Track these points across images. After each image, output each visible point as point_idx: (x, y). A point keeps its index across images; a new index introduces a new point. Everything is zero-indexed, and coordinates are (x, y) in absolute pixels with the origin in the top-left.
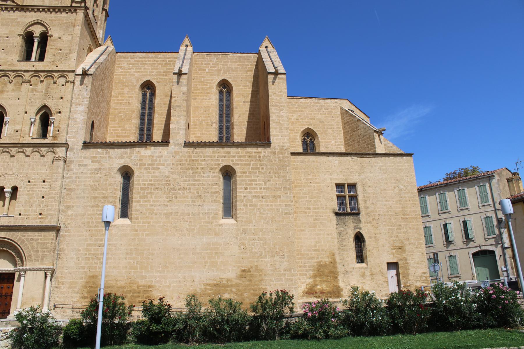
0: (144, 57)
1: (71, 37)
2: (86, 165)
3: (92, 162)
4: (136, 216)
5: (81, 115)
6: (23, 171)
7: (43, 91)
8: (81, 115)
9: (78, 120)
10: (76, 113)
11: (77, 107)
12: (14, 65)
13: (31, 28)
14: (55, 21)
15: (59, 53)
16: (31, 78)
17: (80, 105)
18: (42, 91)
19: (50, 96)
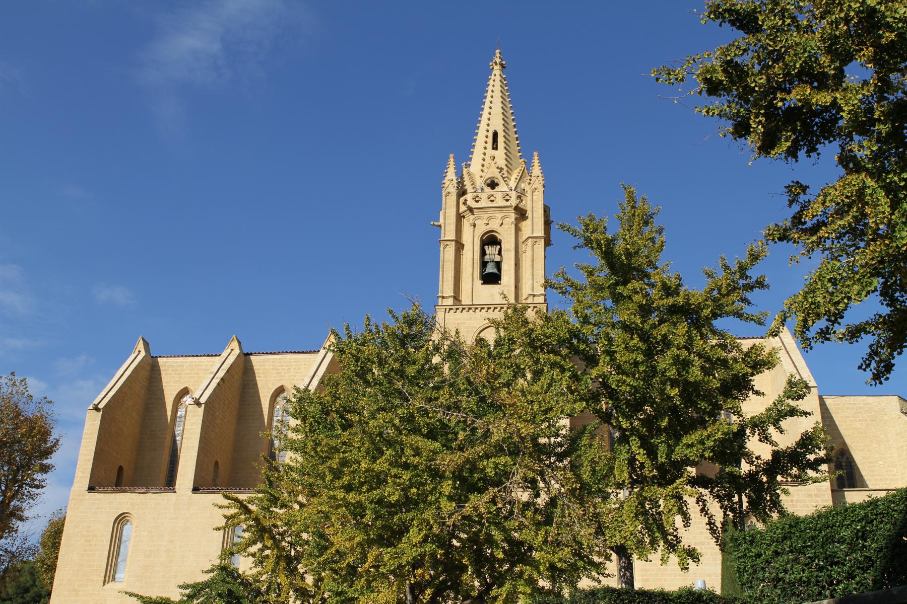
4: (645, 577)
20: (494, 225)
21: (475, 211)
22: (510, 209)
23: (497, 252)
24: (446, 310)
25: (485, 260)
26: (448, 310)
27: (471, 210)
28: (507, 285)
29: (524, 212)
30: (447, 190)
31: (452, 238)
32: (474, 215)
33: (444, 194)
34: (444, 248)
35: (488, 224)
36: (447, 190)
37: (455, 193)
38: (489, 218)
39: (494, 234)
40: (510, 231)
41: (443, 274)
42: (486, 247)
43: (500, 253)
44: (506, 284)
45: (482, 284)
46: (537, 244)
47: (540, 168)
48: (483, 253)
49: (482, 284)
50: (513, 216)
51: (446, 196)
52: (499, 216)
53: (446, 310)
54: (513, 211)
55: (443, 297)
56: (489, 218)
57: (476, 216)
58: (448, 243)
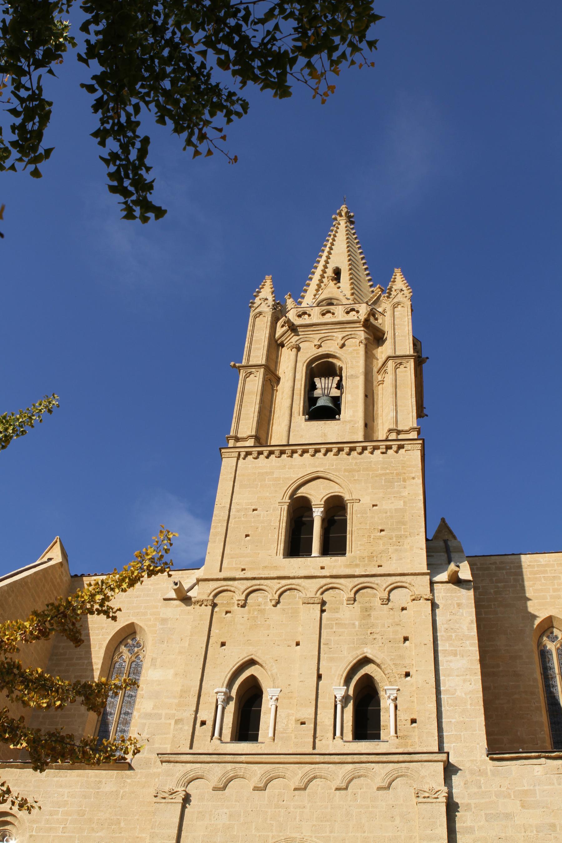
0: (528, 564)
1: (402, 502)
2: (508, 816)
3: (523, 806)
5: (464, 681)
6: (331, 832)
7: (357, 623)
8: (464, 681)
9: (458, 693)
10: (449, 676)
11: (450, 661)
12: (276, 568)
13: (302, 492)
14: (359, 471)
15: (380, 538)
16: (322, 593)
17: (455, 655)
18: (354, 624)
19: (375, 636)
20: (331, 347)
21: (300, 329)
22: (358, 325)
23: (334, 385)
24: (239, 455)
25: (315, 396)
26: (243, 454)
27: (293, 329)
28: (350, 422)
29: (381, 335)
30: (257, 310)
31: (259, 363)
32: (299, 335)
33: (252, 314)
34: (246, 377)
35: (320, 346)
36: (257, 310)
37: (271, 313)
38: (323, 340)
39: (330, 360)
40: (358, 353)
41: (240, 410)
42: (317, 380)
43: (339, 386)
44: (348, 418)
45: (306, 420)
46: (402, 367)
47: (402, 276)
48: (311, 387)
49: (306, 420)
50: (361, 335)
51: (255, 317)
52: (340, 335)
53: (239, 455)
54: (362, 329)
55: (237, 439)
56: (323, 340)
57: (301, 337)
58: (253, 370)
